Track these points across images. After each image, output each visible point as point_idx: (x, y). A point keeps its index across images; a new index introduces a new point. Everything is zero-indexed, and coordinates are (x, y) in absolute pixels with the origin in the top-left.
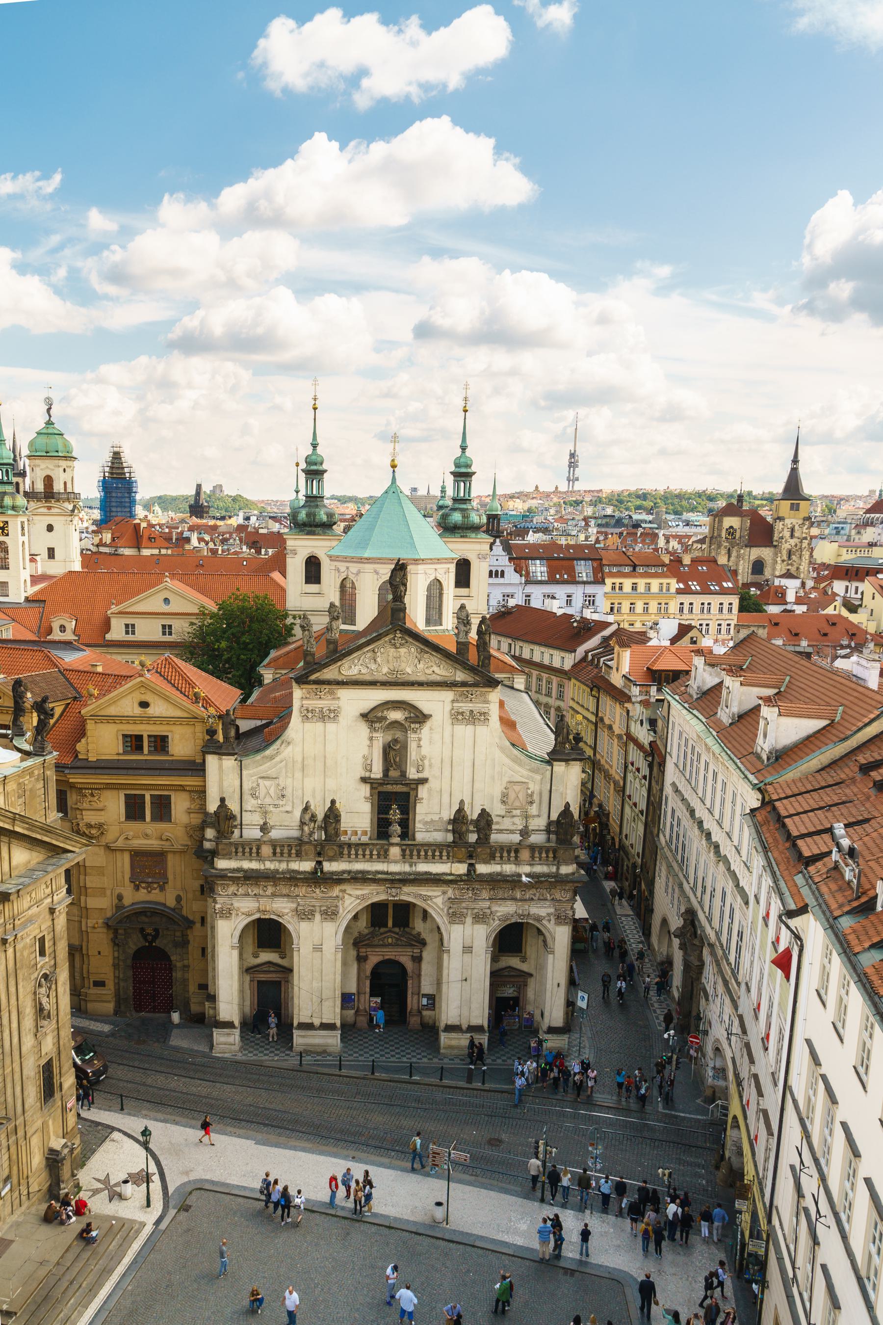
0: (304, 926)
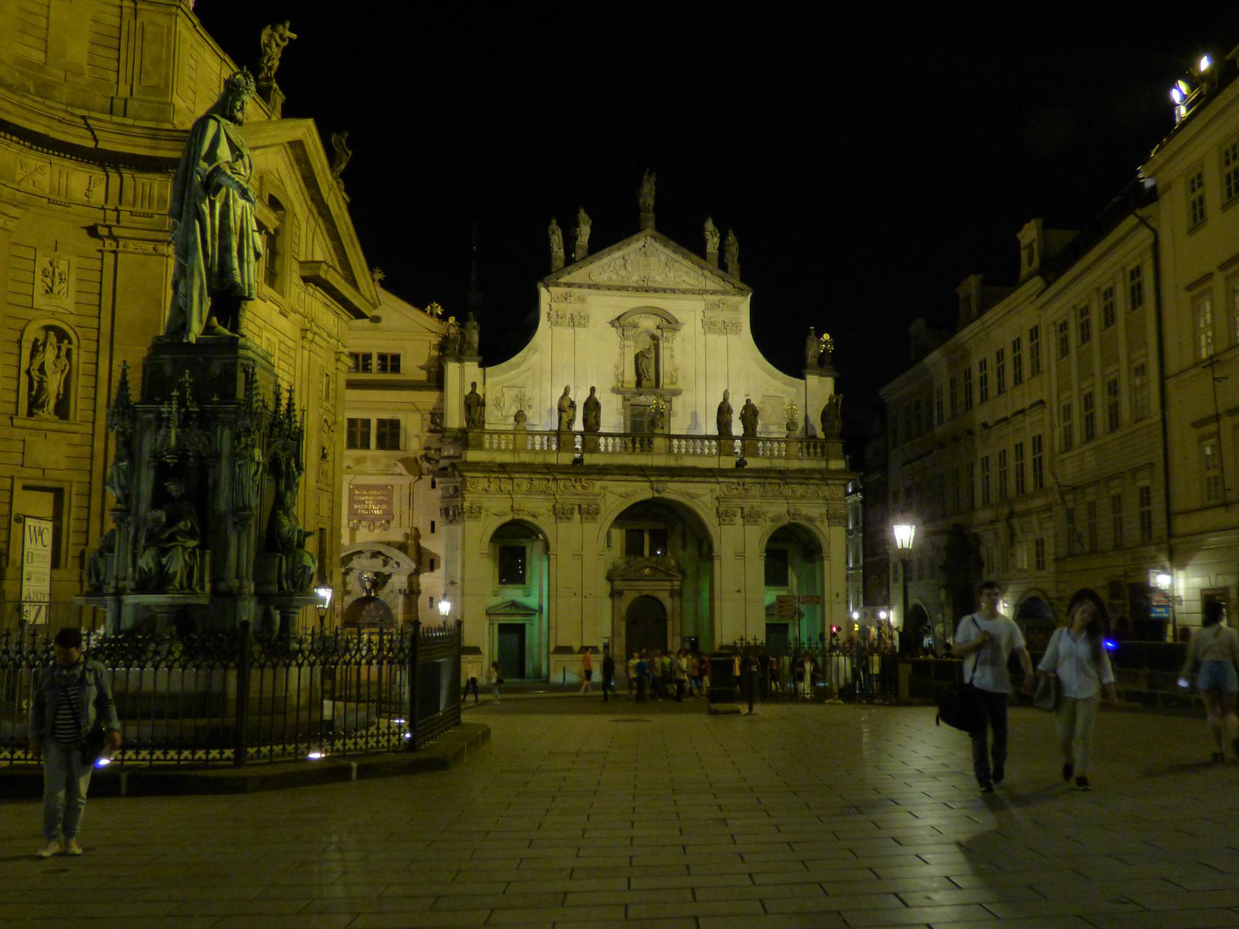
0: (562, 525)
